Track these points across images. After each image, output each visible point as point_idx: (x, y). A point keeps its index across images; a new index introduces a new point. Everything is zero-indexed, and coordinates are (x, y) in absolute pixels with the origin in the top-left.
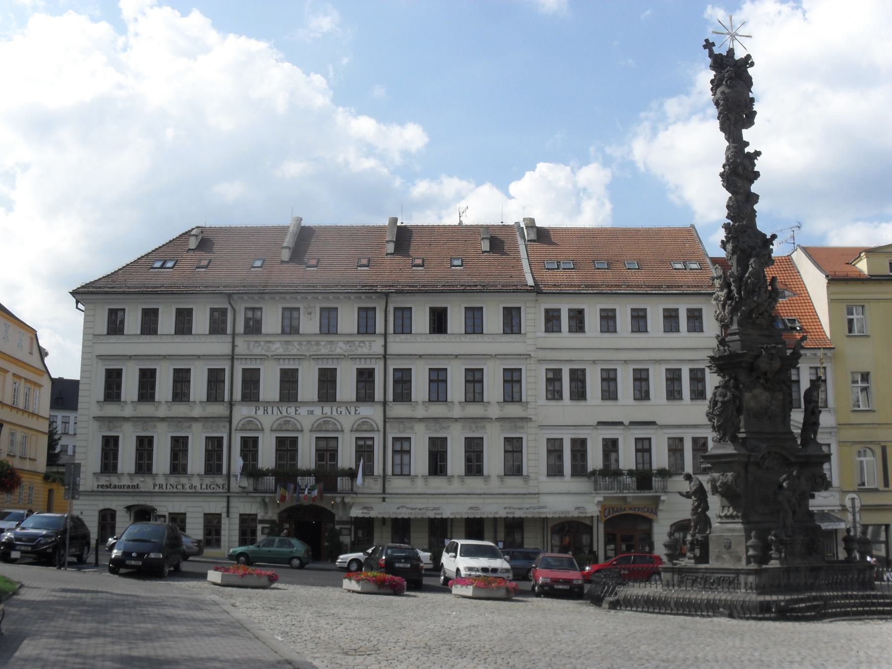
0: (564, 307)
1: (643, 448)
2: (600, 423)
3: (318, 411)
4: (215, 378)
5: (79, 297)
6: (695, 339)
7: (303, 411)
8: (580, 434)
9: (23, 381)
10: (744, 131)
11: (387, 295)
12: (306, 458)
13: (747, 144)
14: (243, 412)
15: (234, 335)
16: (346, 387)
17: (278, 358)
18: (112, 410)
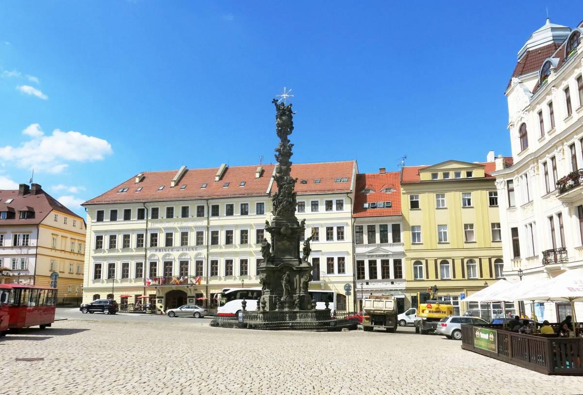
5: (86, 206)
9: (77, 241)
10: (288, 136)
11: (207, 200)
12: (176, 271)
13: (289, 141)
16: (192, 239)
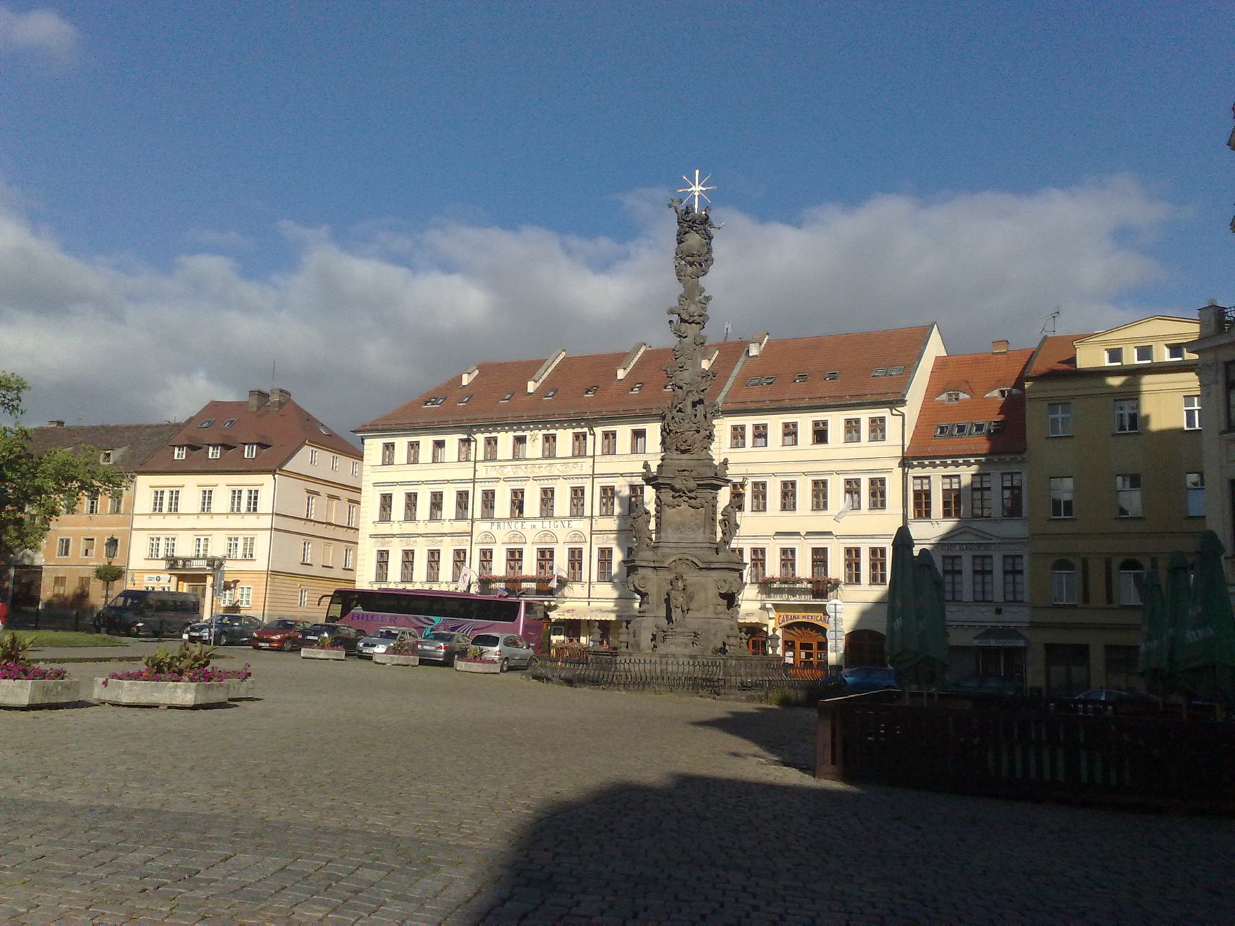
0: (749, 422)
1: (820, 557)
2: (778, 534)
3: (539, 524)
4: (462, 498)
6: (877, 448)
7: (528, 525)
8: (759, 544)
12: (529, 567)
14: (482, 527)
15: (475, 462)
16: (562, 503)
17: (506, 480)
18: (384, 528)
